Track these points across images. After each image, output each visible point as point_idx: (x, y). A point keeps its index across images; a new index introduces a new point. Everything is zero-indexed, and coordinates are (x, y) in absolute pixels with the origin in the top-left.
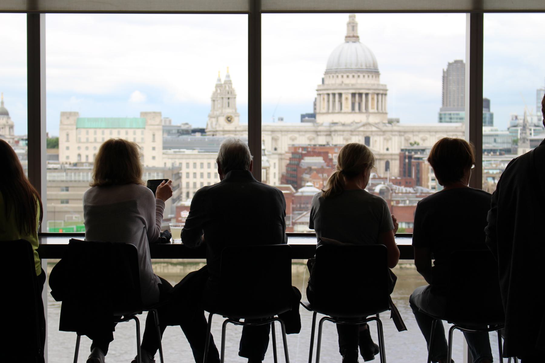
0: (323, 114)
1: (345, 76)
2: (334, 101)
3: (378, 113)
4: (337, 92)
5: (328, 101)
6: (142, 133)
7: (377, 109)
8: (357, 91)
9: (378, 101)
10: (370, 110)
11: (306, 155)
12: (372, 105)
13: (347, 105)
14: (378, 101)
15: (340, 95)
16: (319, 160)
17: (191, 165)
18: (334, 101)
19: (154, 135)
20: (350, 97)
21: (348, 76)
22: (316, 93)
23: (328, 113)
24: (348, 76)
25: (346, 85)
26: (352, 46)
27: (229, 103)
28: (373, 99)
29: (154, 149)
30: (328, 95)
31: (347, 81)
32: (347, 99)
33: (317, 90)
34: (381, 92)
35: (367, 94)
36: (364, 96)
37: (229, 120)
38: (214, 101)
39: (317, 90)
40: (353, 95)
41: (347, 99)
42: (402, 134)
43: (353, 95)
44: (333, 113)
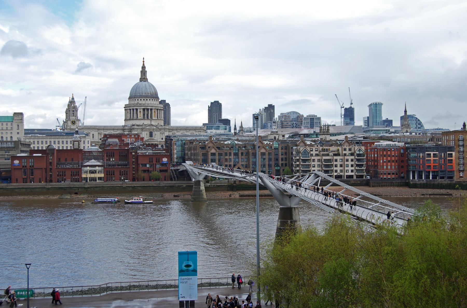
0: (128, 120)
1: (139, 99)
2: (133, 113)
3: (158, 119)
4: (135, 108)
5: (130, 113)
6: (12, 125)
7: (157, 117)
8: (146, 108)
9: (158, 113)
10: (153, 118)
11: (109, 138)
12: (155, 115)
13: (140, 115)
14: (158, 113)
15: (137, 109)
16: (116, 140)
17: (40, 143)
18: (133, 113)
19: (18, 126)
20: (142, 110)
21: (141, 100)
22: (124, 109)
23: (130, 120)
24: (141, 100)
25: (141, 104)
26: (143, 83)
27: (73, 113)
28: (155, 112)
29: (18, 133)
30: (130, 109)
31: (140, 102)
32: (140, 112)
33: (124, 108)
34: (159, 108)
35: (151, 109)
36: (150, 110)
37: (74, 123)
38: (66, 113)
39: (124, 108)
40: (144, 109)
41: (140, 112)
42: (171, 131)
43: (144, 109)
44: (133, 119)
